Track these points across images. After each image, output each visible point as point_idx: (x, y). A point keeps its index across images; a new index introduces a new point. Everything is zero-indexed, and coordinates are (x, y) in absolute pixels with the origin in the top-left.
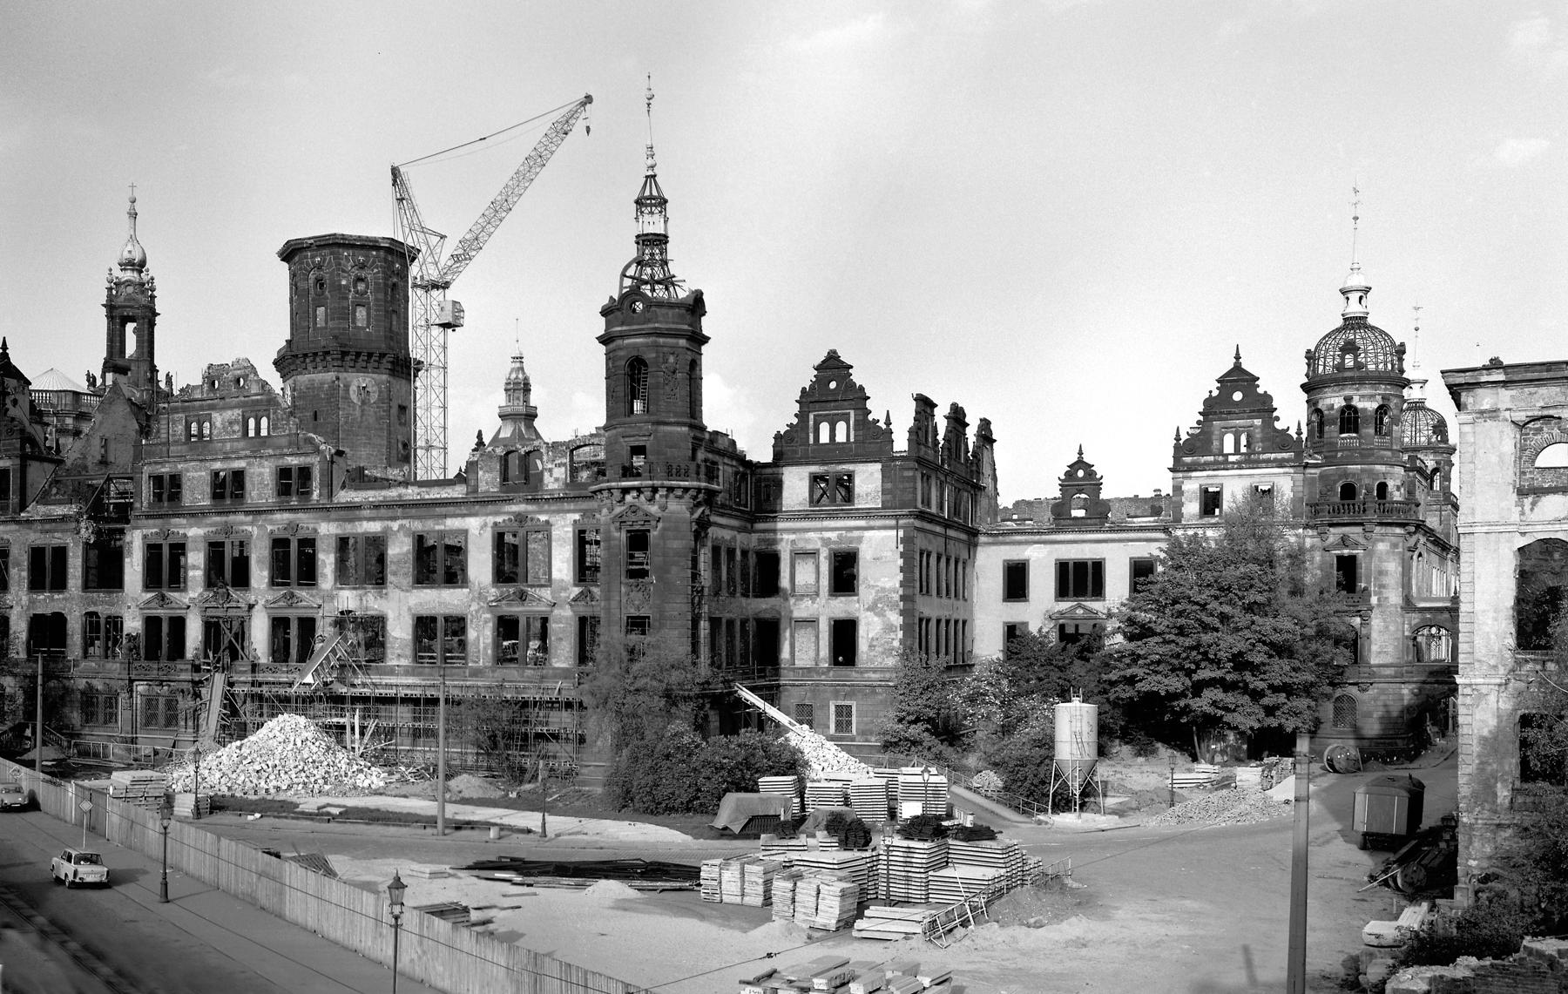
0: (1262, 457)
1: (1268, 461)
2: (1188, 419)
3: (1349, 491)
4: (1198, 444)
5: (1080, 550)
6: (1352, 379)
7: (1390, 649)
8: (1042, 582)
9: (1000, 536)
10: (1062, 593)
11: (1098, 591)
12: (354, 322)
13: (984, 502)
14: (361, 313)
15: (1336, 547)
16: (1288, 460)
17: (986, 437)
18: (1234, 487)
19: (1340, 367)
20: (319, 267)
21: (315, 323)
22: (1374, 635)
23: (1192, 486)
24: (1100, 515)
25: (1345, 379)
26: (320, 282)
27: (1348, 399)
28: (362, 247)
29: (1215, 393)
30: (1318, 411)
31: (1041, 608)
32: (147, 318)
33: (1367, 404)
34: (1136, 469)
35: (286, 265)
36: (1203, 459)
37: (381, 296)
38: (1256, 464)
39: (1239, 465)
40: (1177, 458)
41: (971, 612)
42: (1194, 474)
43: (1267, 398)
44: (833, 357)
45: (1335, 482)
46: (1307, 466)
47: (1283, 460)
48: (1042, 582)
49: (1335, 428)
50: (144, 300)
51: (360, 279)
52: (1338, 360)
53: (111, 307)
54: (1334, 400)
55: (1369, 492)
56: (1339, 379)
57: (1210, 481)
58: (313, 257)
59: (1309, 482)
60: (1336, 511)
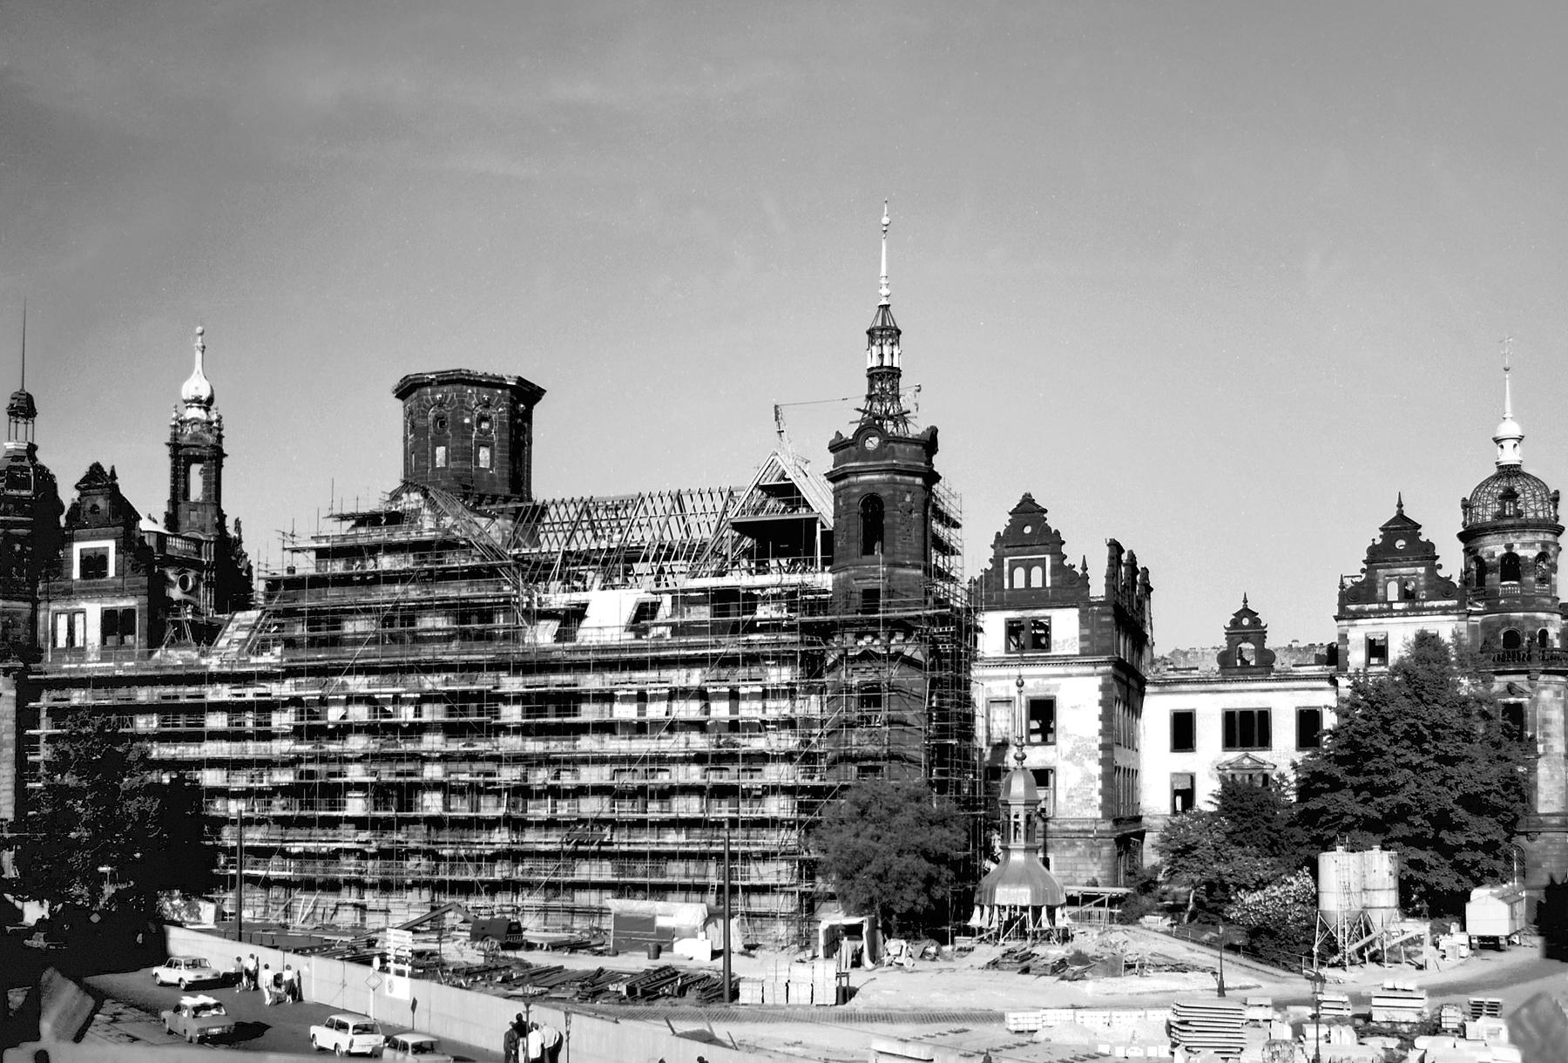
0: (1427, 604)
1: (1432, 609)
2: (1354, 567)
3: (1512, 638)
4: (1363, 592)
5: (1246, 698)
6: (1512, 526)
7: (1556, 799)
8: (1209, 732)
9: (1165, 685)
10: (1229, 743)
11: (1265, 742)
12: (477, 462)
13: (1147, 651)
14: (484, 454)
15: (1502, 694)
16: (1452, 608)
17: (1149, 589)
18: (1400, 634)
19: (1500, 516)
20: (440, 404)
21: (434, 463)
22: (1541, 784)
23: (1359, 632)
24: (1265, 665)
25: (1508, 527)
26: (440, 420)
27: (1509, 547)
28: (488, 385)
29: (1379, 541)
30: (1479, 560)
31: (1209, 759)
32: (215, 458)
33: (1527, 551)
34: (1301, 618)
35: (400, 403)
36: (1367, 607)
37: (506, 436)
38: (1419, 611)
39: (1404, 613)
40: (1342, 606)
41: (1138, 761)
42: (1359, 622)
43: (1430, 546)
44: (1027, 500)
45: (1498, 629)
46: (1470, 614)
47: (1447, 608)
48: (1209, 732)
49: (1496, 576)
50: (211, 439)
51: (482, 419)
52: (1498, 508)
53: (175, 447)
54: (1494, 548)
55: (1533, 639)
56: (1496, 529)
57: (1375, 629)
58: (433, 394)
59: (1472, 629)
60: (1502, 659)
